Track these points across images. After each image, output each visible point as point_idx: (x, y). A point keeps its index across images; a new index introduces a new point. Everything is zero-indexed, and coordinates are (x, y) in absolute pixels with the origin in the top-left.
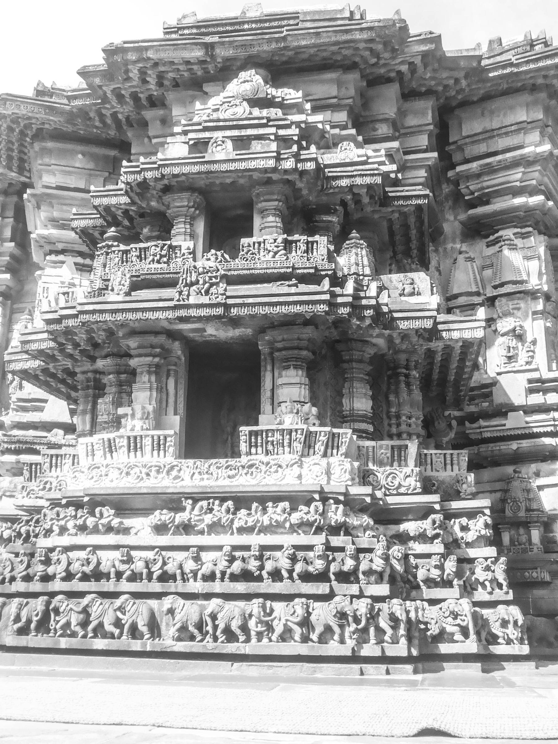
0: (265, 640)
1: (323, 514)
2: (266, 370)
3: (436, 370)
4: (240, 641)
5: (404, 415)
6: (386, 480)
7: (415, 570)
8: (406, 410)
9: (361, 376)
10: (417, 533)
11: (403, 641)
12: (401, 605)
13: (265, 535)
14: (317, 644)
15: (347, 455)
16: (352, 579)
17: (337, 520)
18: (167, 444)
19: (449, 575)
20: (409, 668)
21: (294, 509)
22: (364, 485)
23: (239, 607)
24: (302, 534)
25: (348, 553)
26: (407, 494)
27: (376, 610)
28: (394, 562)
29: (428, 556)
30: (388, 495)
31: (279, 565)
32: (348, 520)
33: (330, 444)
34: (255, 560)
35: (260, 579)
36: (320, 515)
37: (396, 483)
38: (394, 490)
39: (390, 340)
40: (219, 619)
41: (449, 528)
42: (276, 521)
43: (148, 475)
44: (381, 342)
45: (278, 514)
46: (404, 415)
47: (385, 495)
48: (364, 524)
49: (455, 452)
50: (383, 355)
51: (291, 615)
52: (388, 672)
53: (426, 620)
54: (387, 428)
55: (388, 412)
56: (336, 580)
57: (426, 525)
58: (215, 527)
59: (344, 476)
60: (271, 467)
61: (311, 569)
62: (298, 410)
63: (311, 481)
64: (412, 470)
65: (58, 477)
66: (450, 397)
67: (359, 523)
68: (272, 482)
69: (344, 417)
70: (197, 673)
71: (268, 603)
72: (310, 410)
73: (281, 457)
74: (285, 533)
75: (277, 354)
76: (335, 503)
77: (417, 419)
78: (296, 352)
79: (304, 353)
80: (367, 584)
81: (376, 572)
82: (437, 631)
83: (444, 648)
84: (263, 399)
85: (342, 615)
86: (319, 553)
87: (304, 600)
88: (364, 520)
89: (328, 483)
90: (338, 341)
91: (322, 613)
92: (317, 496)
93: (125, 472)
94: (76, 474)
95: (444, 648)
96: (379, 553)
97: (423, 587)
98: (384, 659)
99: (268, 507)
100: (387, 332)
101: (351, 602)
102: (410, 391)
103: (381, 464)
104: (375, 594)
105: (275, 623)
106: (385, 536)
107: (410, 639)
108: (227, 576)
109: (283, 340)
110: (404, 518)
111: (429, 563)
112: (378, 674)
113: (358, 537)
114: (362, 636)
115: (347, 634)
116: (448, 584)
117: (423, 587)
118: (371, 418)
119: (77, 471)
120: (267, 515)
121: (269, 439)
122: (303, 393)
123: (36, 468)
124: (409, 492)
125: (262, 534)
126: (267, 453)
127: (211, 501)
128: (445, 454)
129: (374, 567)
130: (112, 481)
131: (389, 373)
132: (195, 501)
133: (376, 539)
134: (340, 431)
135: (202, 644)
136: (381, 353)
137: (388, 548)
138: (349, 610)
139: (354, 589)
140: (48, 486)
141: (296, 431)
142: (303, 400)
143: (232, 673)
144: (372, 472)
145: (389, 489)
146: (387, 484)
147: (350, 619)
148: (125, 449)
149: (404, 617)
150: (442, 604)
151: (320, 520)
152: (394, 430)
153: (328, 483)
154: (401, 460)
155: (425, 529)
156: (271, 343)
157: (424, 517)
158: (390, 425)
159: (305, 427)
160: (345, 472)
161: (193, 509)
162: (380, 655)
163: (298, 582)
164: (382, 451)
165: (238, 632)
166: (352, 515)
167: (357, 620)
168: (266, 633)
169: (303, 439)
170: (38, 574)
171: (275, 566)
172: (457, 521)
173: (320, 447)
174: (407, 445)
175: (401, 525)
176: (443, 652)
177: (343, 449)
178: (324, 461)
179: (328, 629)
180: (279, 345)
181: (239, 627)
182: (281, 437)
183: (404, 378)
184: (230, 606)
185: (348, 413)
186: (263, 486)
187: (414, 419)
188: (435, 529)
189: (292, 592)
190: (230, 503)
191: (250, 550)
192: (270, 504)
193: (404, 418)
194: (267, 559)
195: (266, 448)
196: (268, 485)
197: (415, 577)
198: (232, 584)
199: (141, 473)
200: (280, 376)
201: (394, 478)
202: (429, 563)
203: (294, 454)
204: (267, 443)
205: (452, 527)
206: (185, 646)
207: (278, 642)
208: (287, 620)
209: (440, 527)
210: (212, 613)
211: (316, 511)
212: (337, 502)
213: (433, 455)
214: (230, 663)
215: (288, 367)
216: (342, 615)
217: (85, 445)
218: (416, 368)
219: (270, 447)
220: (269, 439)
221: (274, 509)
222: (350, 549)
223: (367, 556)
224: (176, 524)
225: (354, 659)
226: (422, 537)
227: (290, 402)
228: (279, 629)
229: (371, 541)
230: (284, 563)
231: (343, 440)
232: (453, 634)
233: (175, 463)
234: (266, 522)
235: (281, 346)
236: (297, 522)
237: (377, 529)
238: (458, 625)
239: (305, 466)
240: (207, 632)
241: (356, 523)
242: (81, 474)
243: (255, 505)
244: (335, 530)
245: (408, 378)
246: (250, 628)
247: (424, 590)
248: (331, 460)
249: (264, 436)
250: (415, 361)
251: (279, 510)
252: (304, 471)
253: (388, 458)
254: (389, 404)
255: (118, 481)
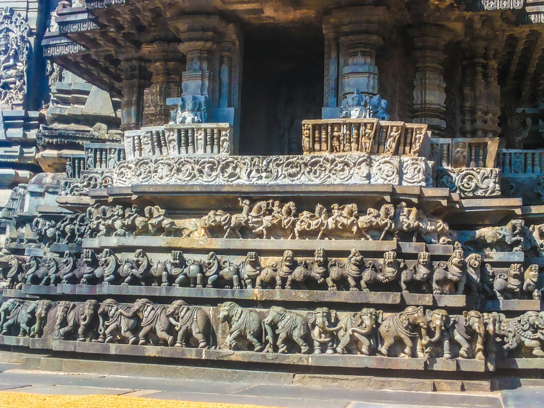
0: (329, 351)
1: (395, 218)
2: (330, 57)
3: (516, 60)
4: (303, 351)
5: (481, 110)
6: (462, 182)
7: (491, 280)
8: (482, 105)
9: (436, 65)
10: (495, 240)
11: (480, 355)
12: (479, 318)
13: (330, 239)
14: (386, 357)
15: (420, 153)
16: (424, 288)
17: (409, 224)
18: (222, 138)
19: (529, 285)
20: (486, 384)
21: (362, 212)
22: (437, 187)
23: (301, 316)
24: (370, 239)
25: (421, 260)
26: (484, 197)
27: (452, 322)
28: (470, 271)
29: (507, 264)
30: (464, 198)
31: (346, 272)
32: (421, 225)
33: (402, 140)
34: (319, 266)
35: (324, 286)
36: (391, 218)
37: (473, 185)
38: (469, 192)
39: (469, 25)
40: (280, 327)
41: (527, 235)
42: (343, 225)
43: (200, 171)
44: (459, 27)
45: (345, 217)
46: (481, 110)
47: (461, 198)
48: (439, 229)
49: (530, 151)
50: (458, 43)
51: (359, 326)
52: (463, 389)
53: (502, 332)
54: (459, 124)
55: (462, 107)
56: (406, 289)
57: (505, 231)
58: (274, 231)
59: (417, 176)
60: (336, 165)
61: (380, 277)
62: (366, 102)
63: (381, 181)
64: (491, 171)
65: (103, 173)
66: (526, 91)
67: (433, 227)
68: (338, 181)
69: (414, 111)
70: (256, 385)
71: (333, 313)
72: (379, 103)
73: (348, 154)
74: (352, 238)
75: (343, 38)
76: (407, 206)
77: (494, 115)
78: (365, 36)
79: (374, 38)
80: (441, 294)
81: (451, 281)
82: (515, 345)
83: (522, 363)
84: (326, 90)
85: (414, 327)
86: (389, 260)
87: (372, 310)
88: (438, 224)
89: (400, 183)
90: (410, 26)
91: (392, 324)
92: (388, 198)
93: (175, 168)
94: (122, 170)
95: (522, 363)
96: (456, 260)
97: (501, 298)
98: (459, 375)
99: (333, 209)
100: (468, 14)
101: (424, 313)
102: (488, 84)
103: (456, 163)
104: (449, 305)
105: (341, 333)
106: (459, 242)
107: (486, 352)
108: (288, 283)
109: (350, 23)
110: (480, 223)
111: (507, 272)
112: (452, 391)
113: (431, 243)
114: (436, 349)
115: (419, 347)
116: (527, 295)
117: (501, 298)
118: (444, 113)
119: (124, 167)
120: (334, 217)
121: (335, 134)
122: (371, 83)
123: (79, 163)
124: (487, 195)
125: (327, 239)
126: (332, 149)
127: (271, 201)
128: (526, 154)
129: (450, 276)
130: (161, 178)
131: (465, 62)
132: (253, 201)
133: (452, 246)
134: (415, 126)
135: (261, 353)
136: (456, 40)
137: (465, 256)
138: (421, 322)
139: (427, 299)
140: (92, 182)
141: (365, 125)
142: (371, 91)
143: (293, 385)
144: (445, 173)
145: (464, 192)
146: (463, 186)
147: (423, 331)
148: (175, 143)
149: (482, 331)
150: (522, 316)
151: (391, 224)
152: (468, 127)
153: (400, 183)
154: (479, 159)
155: (504, 236)
156: (336, 27)
157: (502, 222)
158: (463, 122)
159: (375, 120)
160: (419, 172)
161: (250, 210)
162: (455, 370)
163: (366, 290)
164: (459, 149)
165: (300, 342)
166: (426, 219)
167: (430, 333)
168: (330, 344)
169: (372, 135)
170: (85, 275)
171: (340, 273)
172: (537, 227)
173: (391, 144)
174: (487, 143)
175: (477, 231)
176: (520, 367)
177: (417, 146)
178: (396, 160)
179: (399, 342)
180: (346, 29)
181: (302, 337)
182: (348, 132)
183: (481, 68)
184: (292, 314)
185: (419, 107)
186: (328, 185)
187: (490, 115)
188: (515, 235)
189: (360, 302)
190: (291, 204)
191: (314, 256)
192: (336, 206)
193: (479, 114)
194: (332, 266)
195: (331, 143)
196: (334, 185)
197: (491, 286)
198: (293, 292)
199: (193, 169)
200: (346, 64)
201: (470, 179)
202: (507, 272)
203: (362, 151)
204: (333, 137)
205: (531, 233)
206: (243, 355)
207: (343, 353)
208: (354, 331)
209: (522, 233)
210: (272, 321)
211: (387, 215)
212: (410, 204)
213: (513, 155)
214: (292, 374)
215: (355, 55)
216: (414, 327)
217: (132, 139)
218: (495, 57)
219: (336, 143)
220: (335, 134)
221: (340, 211)
222: (424, 255)
223: (442, 265)
224: (232, 225)
225: (427, 373)
226: (501, 245)
227: (358, 93)
228: (345, 340)
229: (447, 247)
230: (351, 270)
231: (418, 136)
232: (532, 349)
233: (230, 159)
234: (331, 226)
235: (349, 30)
236: (365, 226)
237: (451, 234)
238: (538, 339)
239: (375, 164)
240: (267, 342)
241: (430, 228)
242: (127, 170)
243: (319, 207)
244: (407, 235)
245: (486, 69)
246: (314, 338)
247: (501, 301)
248: (404, 158)
249: (329, 130)
250: (494, 49)
251: (345, 213)
252: (374, 170)
253: (464, 157)
254: (463, 98)
255: (168, 178)
